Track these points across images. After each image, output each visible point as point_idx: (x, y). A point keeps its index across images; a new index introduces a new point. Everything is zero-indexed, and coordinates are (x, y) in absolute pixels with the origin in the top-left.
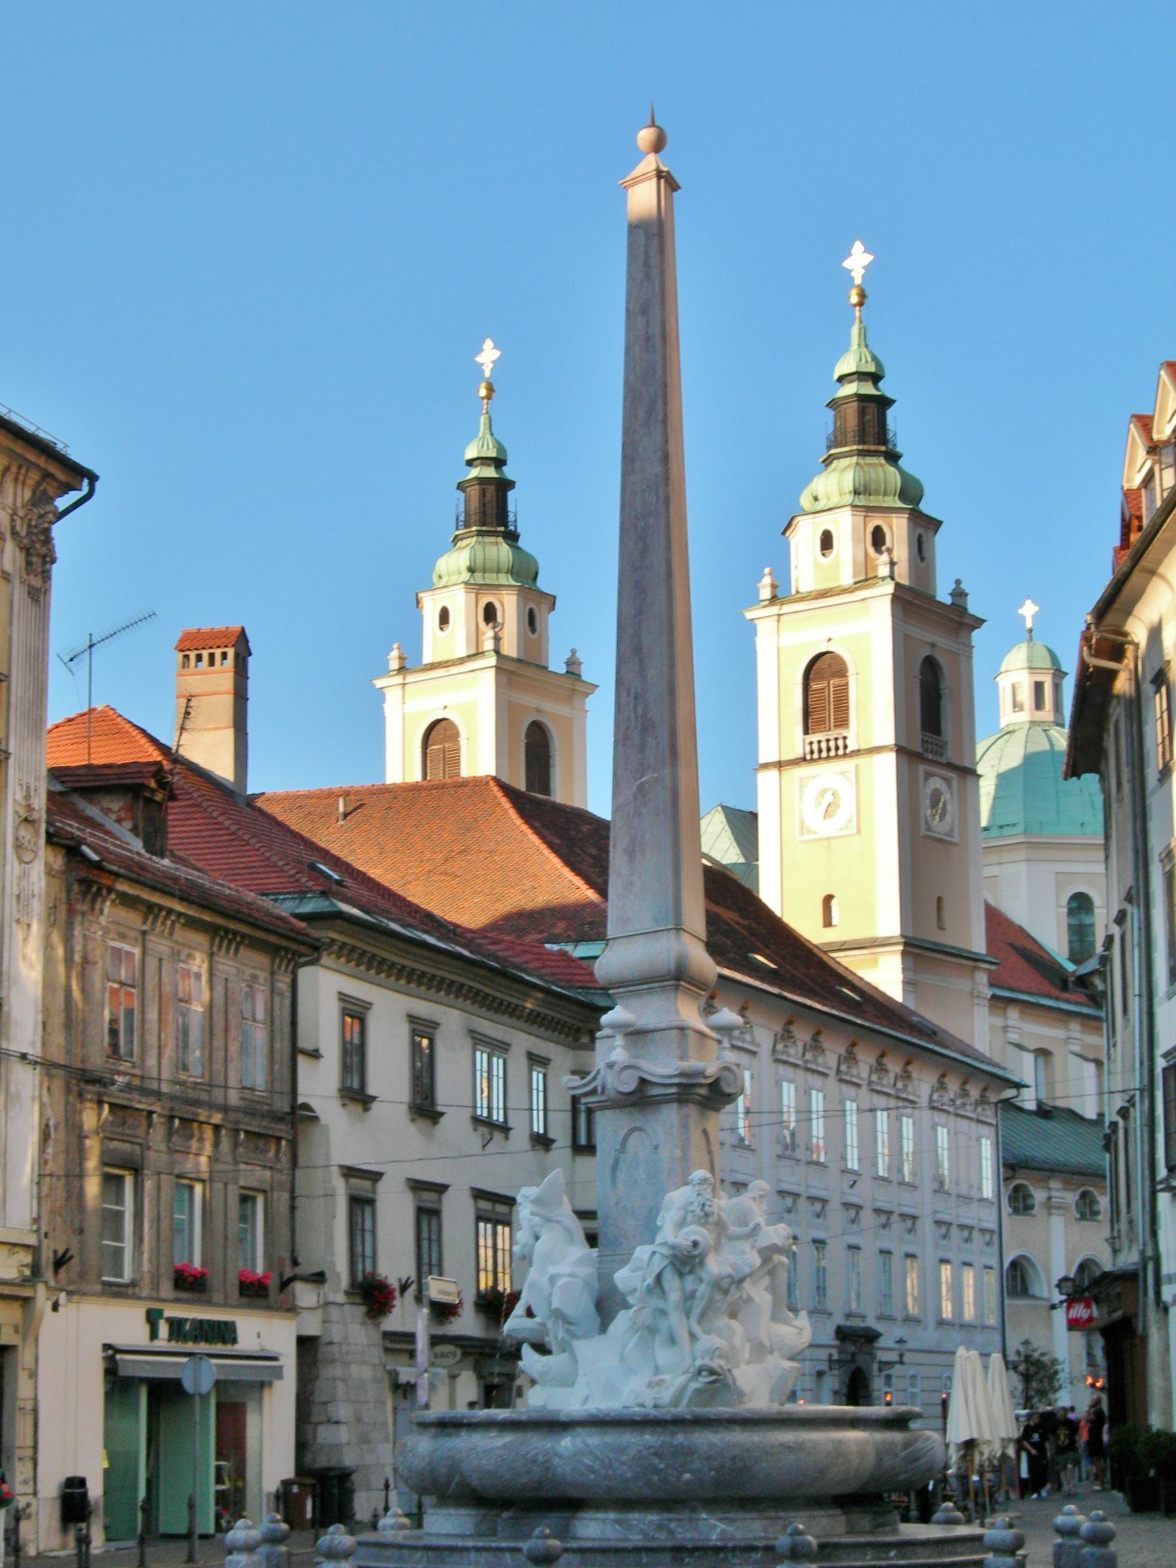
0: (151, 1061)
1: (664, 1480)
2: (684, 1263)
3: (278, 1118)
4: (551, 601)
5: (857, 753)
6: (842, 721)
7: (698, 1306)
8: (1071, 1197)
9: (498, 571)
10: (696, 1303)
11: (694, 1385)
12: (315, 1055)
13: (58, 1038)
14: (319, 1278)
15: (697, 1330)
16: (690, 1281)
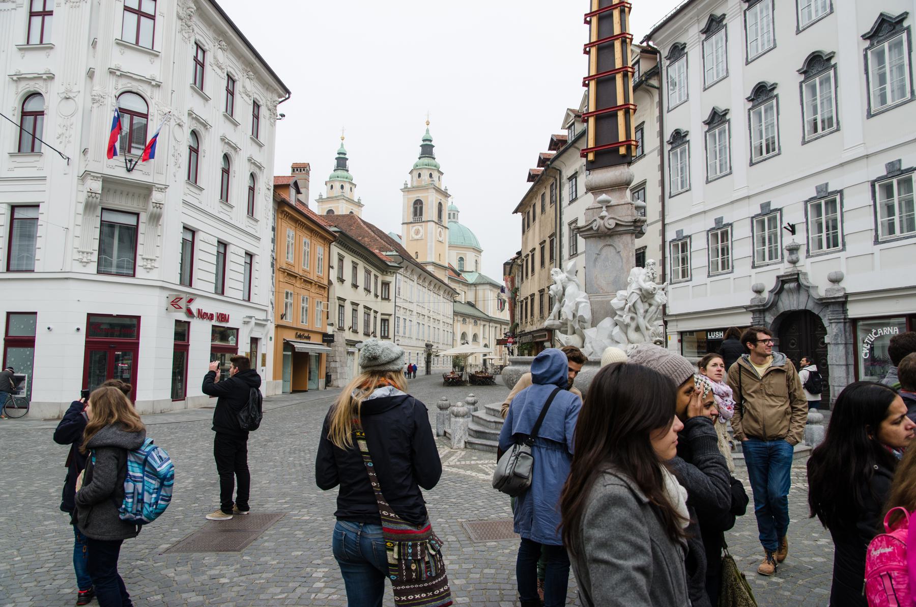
4: (355, 185)
5: (424, 222)
6: (421, 214)
7: (649, 316)
8: (461, 319)
9: (344, 178)
10: (648, 314)
12: (332, 268)
14: (332, 325)
15: (648, 325)
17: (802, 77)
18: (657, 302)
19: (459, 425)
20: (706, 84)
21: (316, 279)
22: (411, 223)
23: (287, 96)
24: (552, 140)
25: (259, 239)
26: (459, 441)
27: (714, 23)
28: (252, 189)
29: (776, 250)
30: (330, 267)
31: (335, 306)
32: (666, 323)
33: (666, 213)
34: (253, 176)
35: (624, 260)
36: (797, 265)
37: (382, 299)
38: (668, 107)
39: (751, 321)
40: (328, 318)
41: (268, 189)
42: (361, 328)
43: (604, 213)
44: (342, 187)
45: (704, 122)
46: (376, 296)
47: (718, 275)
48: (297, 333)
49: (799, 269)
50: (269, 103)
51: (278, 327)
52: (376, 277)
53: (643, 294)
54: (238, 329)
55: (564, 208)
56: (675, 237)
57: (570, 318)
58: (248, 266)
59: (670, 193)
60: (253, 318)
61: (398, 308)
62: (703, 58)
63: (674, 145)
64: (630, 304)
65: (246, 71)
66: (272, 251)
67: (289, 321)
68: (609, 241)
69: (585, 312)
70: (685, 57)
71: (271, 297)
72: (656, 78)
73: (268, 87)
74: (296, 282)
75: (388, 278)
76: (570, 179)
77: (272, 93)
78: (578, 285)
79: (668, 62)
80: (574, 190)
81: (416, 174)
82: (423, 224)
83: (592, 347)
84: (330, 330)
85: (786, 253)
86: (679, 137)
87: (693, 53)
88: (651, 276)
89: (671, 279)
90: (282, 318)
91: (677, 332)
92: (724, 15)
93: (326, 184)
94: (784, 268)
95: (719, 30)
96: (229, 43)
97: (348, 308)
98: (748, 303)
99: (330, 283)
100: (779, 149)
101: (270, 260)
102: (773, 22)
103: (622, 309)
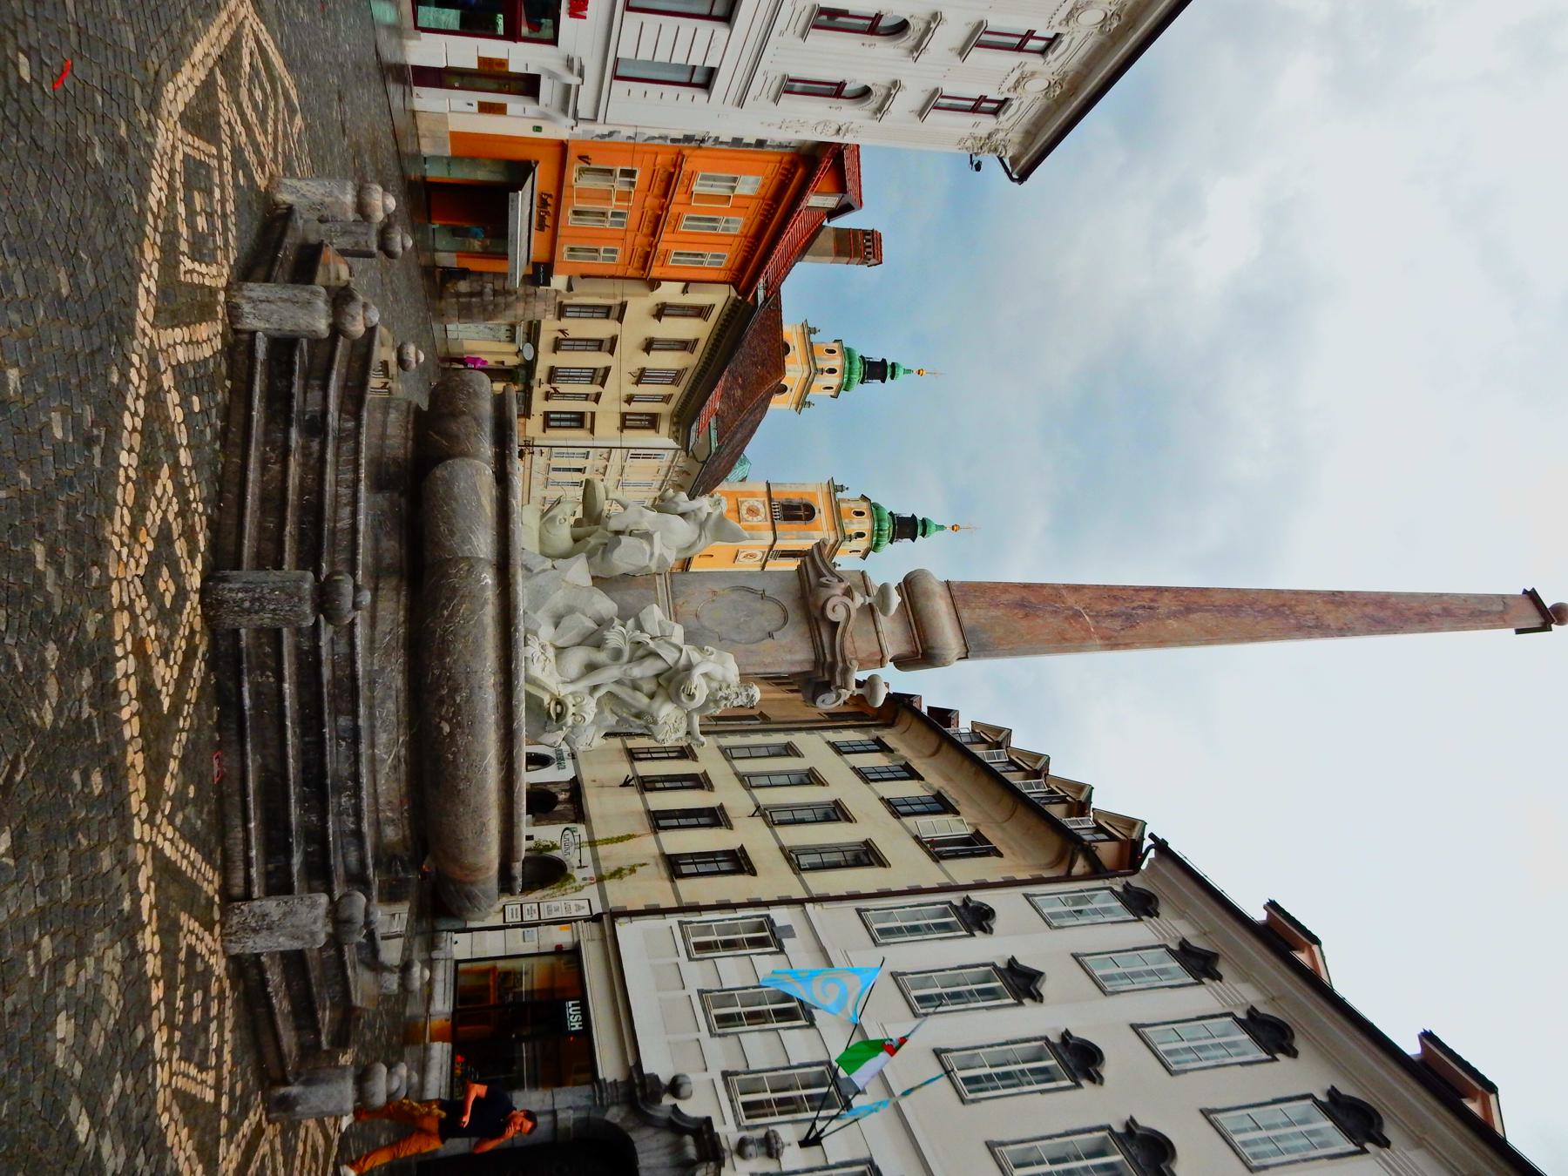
1: (441, 702)
2: (669, 681)
4: (835, 397)
10: (629, 691)
11: (546, 699)
12: (685, 291)
14: (570, 288)
16: (649, 686)
17: (1118, 1129)
18: (659, 709)
19: (336, 192)
20: (1087, 958)
21: (661, 247)
22: (770, 499)
23: (1015, 176)
24: (950, 711)
25: (741, 103)
26: (296, 191)
27: (1202, 963)
28: (836, 91)
29: (765, 1115)
30: (688, 283)
31: (608, 296)
32: (596, 919)
33: (826, 905)
34: (865, 93)
35: (753, 647)
36: (737, 1159)
37: (624, 416)
38: (1035, 895)
39: (610, 1079)
40: (583, 277)
41: (839, 129)
42: (564, 359)
43: (859, 600)
44: (832, 371)
45: (1013, 958)
46: (630, 399)
47: (704, 1010)
48: (550, 196)
49: (728, 1162)
50: (1001, 135)
51: (563, 146)
52: (666, 399)
53: (677, 672)
54: (554, 41)
55: (823, 738)
56: (778, 924)
57: (614, 525)
58: (685, 78)
59: (868, 910)
60: (578, 80)
61: (605, 456)
62: (1135, 949)
63: (962, 911)
64: (652, 644)
65: (1063, 79)
66: (717, 138)
67: (579, 182)
68: (795, 616)
69: (627, 556)
70: (1132, 917)
71: (626, 132)
72: (1088, 869)
73: (1030, 134)
74: (656, 197)
75: (665, 426)
76: (878, 741)
77: (1021, 143)
78: (689, 547)
79: (1119, 889)
80: (857, 748)
81: (863, 507)
82: (769, 523)
83: (544, 571)
84: (558, 282)
85: (760, 1133)
86: (978, 919)
87: (1141, 932)
88: (720, 694)
89: (691, 922)
90: (583, 158)
91: (579, 942)
92: (1220, 978)
94: (727, 1131)
95: (1191, 972)
96: (1115, 38)
97: (600, 329)
98: (646, 1070)
99: (654, 284)
100: (973, 1101)
101: (697, 130)
102: (1218, 1066)
103: (640, 627)
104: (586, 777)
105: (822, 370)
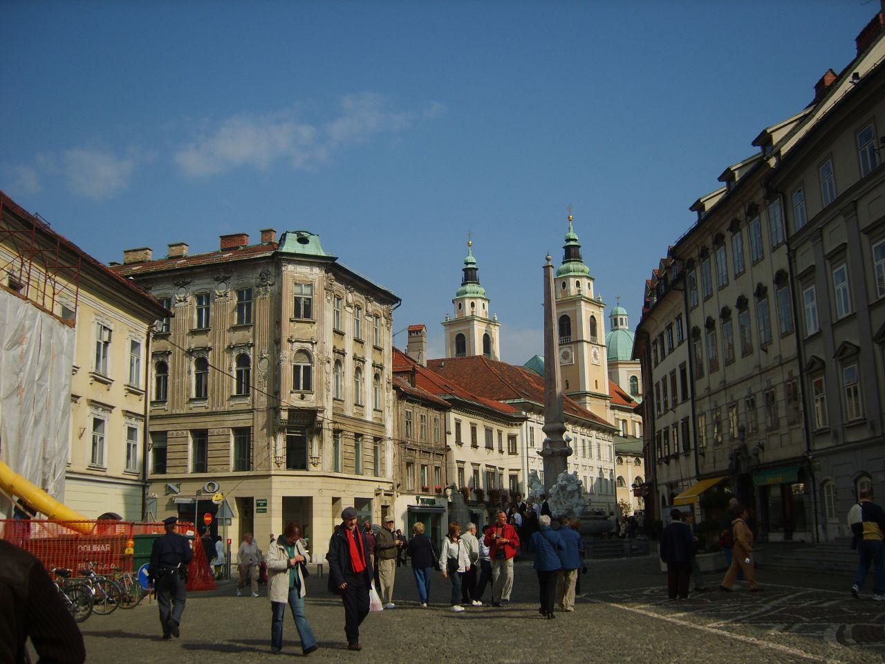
0: (415, 437)
3: (442, 449)
6: (569, 334)
12: (450, 433)
13: (396, 433)
37: (509, 454)
46: (501, 451)
50: (385, 314)
61: (532, 460)
93: (453, 302)
99: (448, 449)
104: (666, 481)
105: (472, 312)
